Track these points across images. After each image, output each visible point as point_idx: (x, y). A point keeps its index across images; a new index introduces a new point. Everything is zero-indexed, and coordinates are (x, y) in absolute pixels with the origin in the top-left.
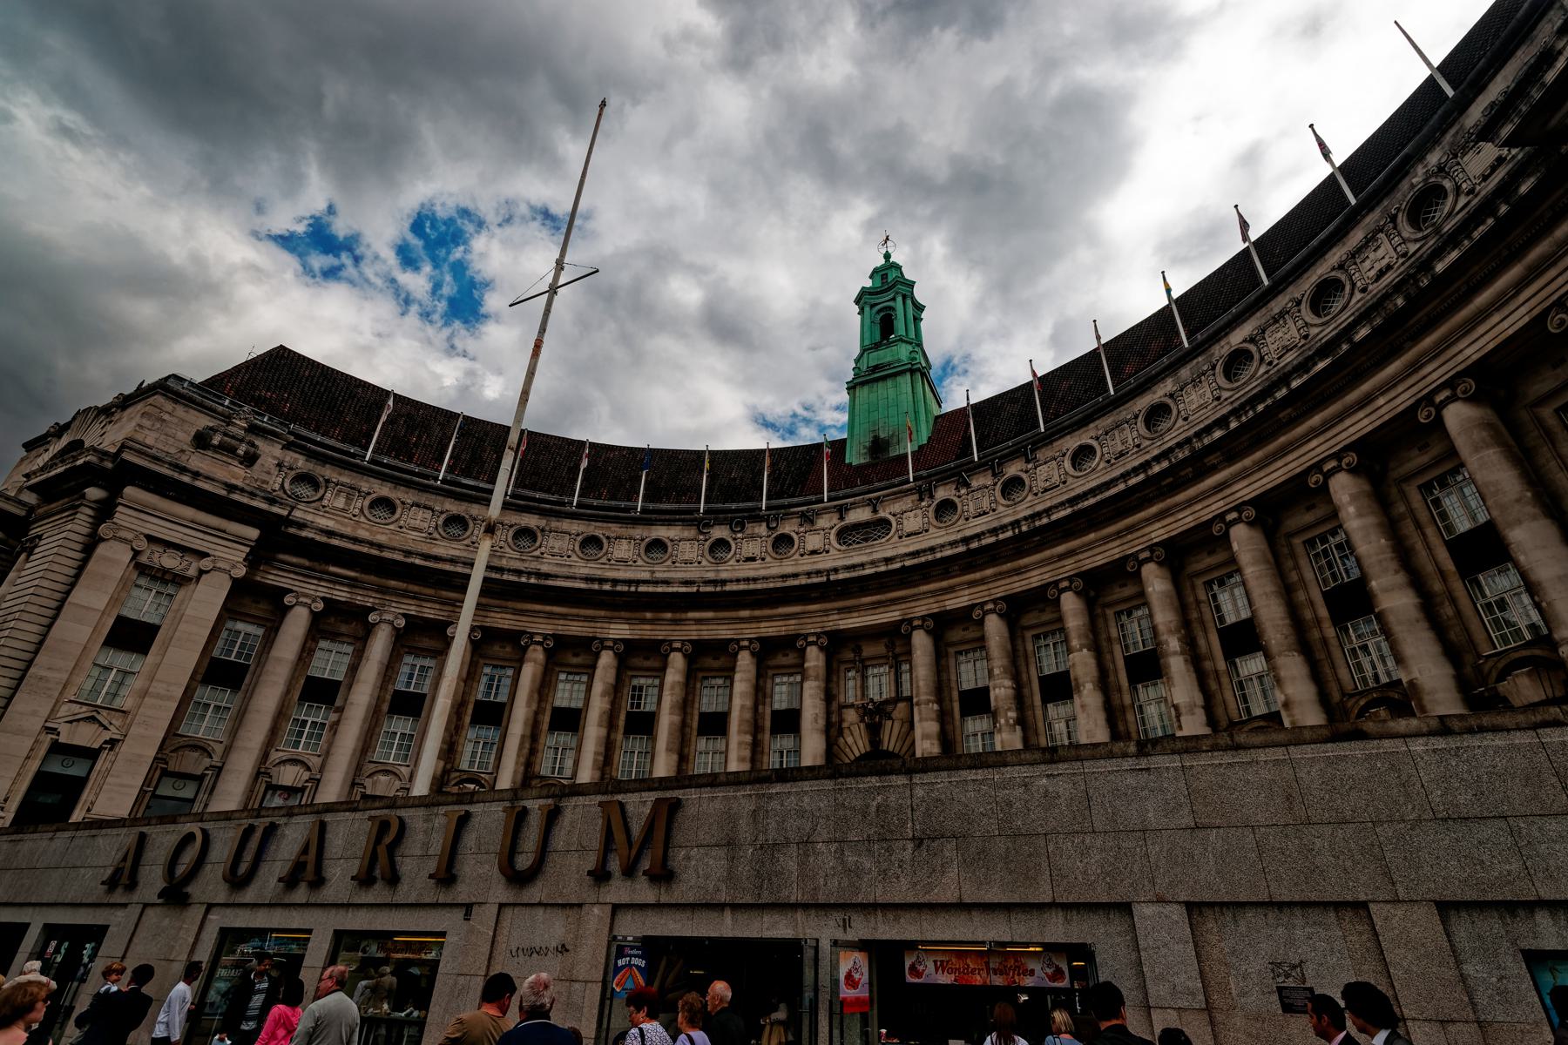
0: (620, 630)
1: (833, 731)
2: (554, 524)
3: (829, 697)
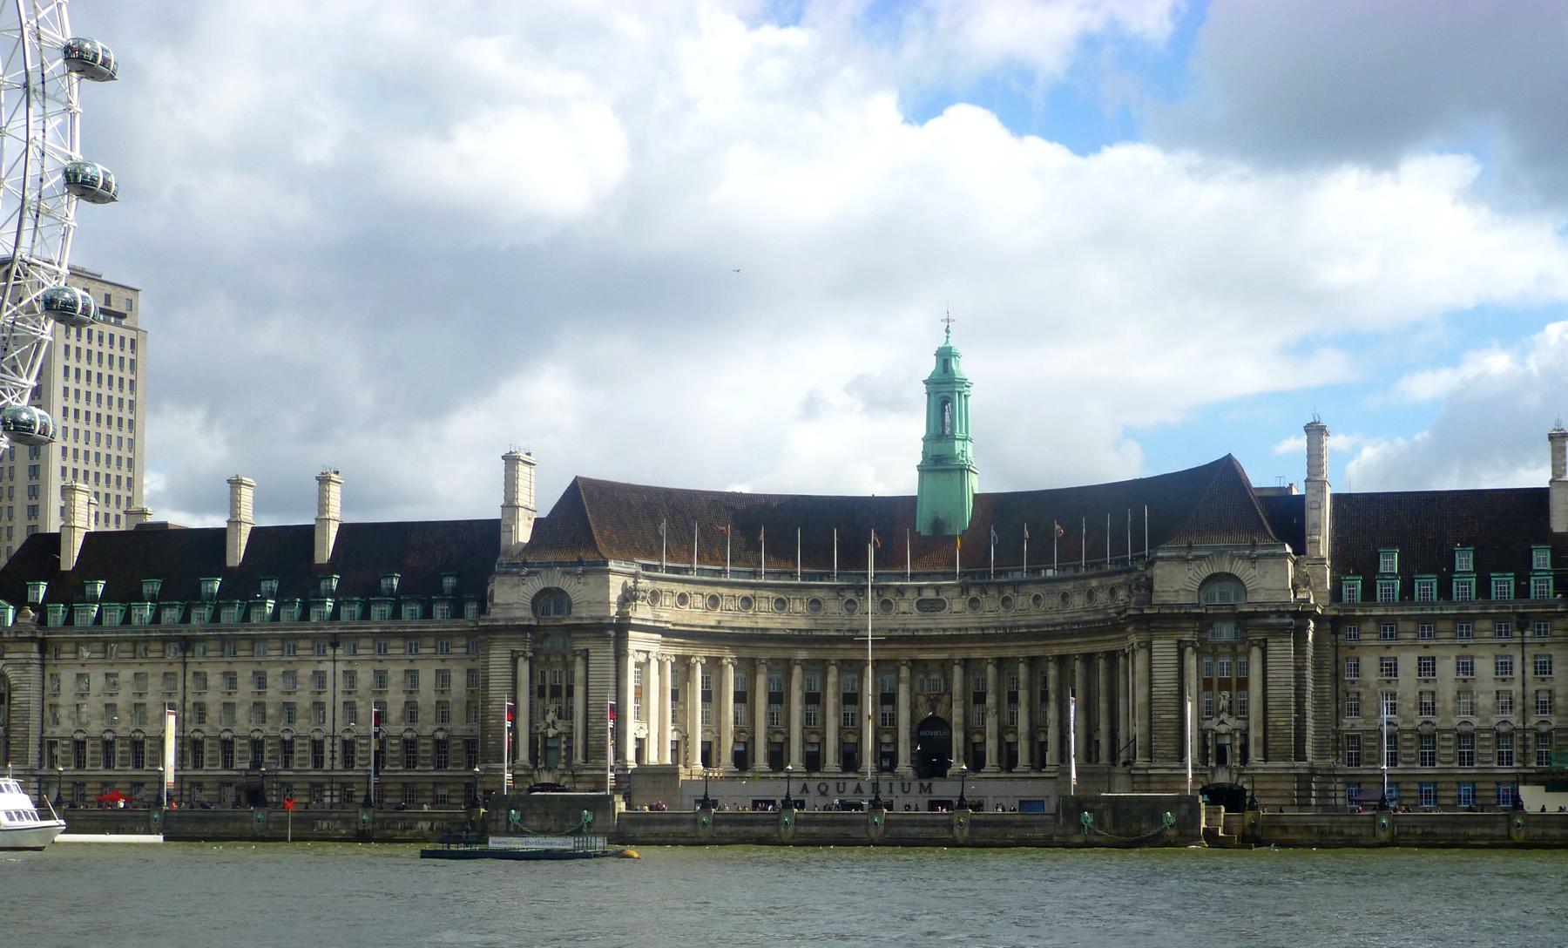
0: (802, 655)
1: (913, 707)
2: (759, 593)
3: (911, 689)
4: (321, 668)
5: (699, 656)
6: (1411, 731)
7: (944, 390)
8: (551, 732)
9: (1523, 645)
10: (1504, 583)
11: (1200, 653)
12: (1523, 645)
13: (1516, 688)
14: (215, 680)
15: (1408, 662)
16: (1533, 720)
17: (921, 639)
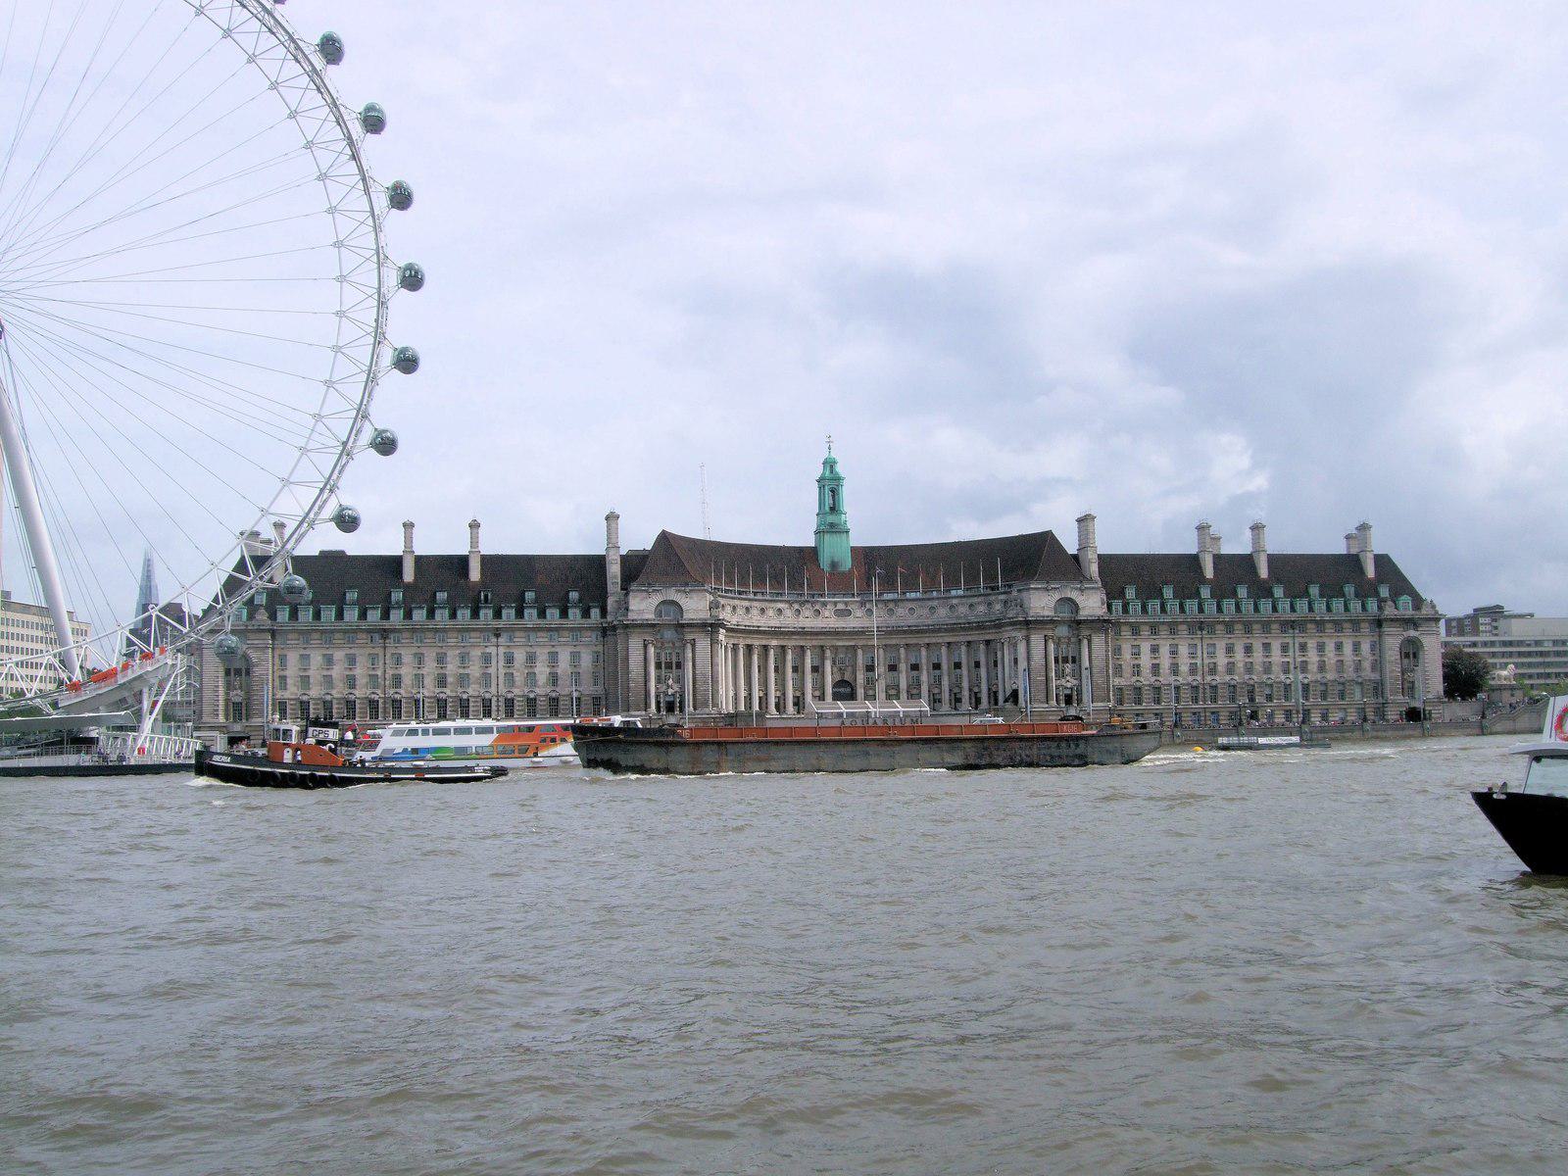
0: (774, 643)
4: (488, 650)
5: (742, 643)
6: (1149, 685)
7: (830, 486)
8: (670, 691)
9: (1202, 639)
10: (1191, 605)
12: (1202, 639)
13: (1199, 662)
15: (1145, 648)
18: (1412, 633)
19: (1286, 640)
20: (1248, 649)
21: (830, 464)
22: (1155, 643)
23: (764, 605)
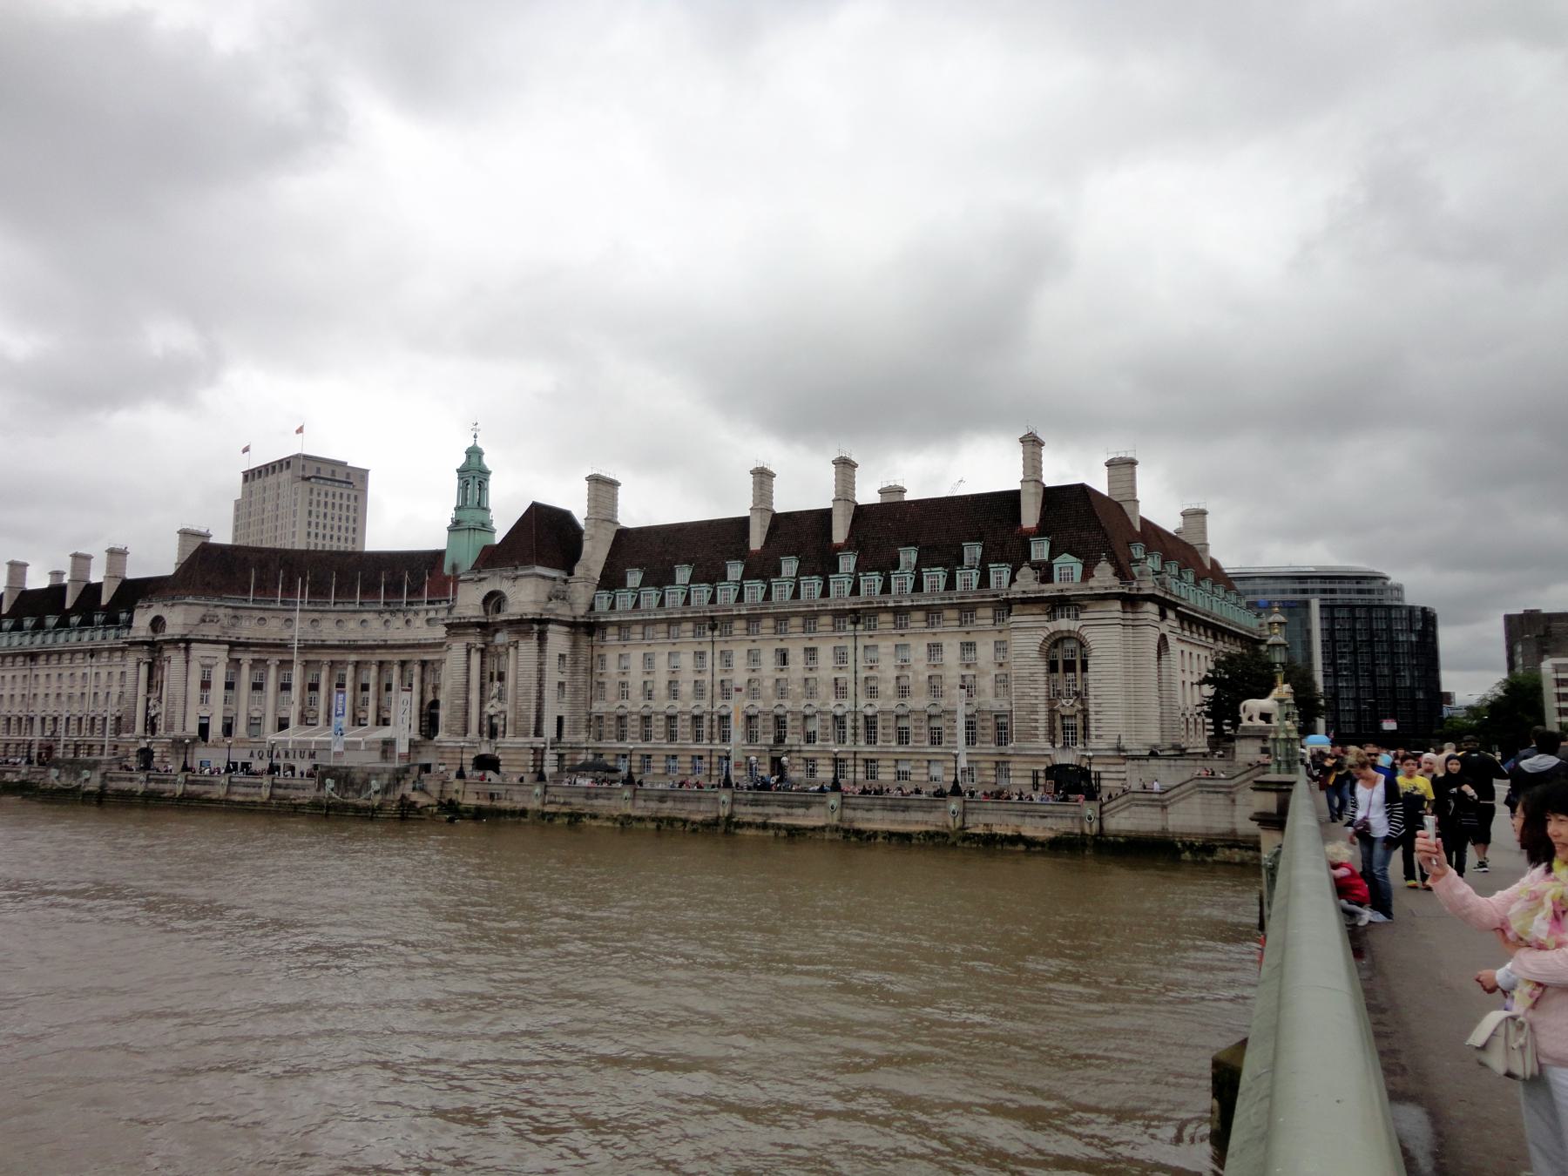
3: (422, 681)
10: (701, 593)
11: (482, 651)
13: (707, 678)
14: (42, 679)
16: (719, 703)
17: (426, 646)
18: (1064, 624)
19: (841, 643)
20: (783, 657)
21: (474, 453)
22: (648, 650)
23: (342, 616)
